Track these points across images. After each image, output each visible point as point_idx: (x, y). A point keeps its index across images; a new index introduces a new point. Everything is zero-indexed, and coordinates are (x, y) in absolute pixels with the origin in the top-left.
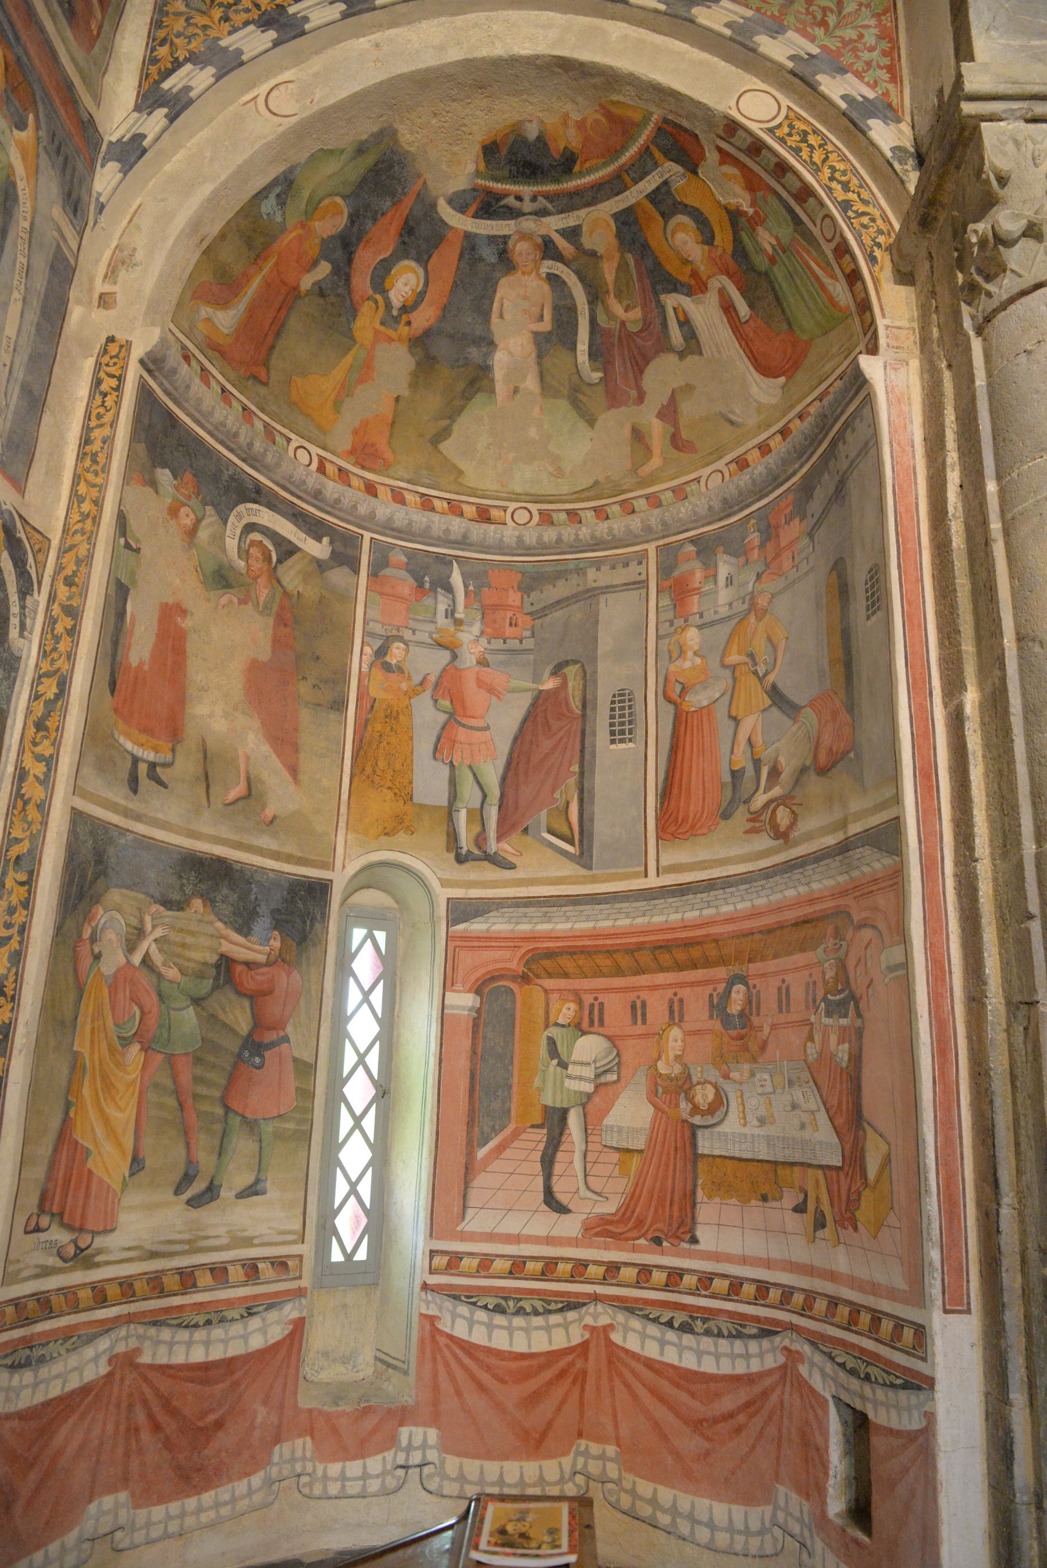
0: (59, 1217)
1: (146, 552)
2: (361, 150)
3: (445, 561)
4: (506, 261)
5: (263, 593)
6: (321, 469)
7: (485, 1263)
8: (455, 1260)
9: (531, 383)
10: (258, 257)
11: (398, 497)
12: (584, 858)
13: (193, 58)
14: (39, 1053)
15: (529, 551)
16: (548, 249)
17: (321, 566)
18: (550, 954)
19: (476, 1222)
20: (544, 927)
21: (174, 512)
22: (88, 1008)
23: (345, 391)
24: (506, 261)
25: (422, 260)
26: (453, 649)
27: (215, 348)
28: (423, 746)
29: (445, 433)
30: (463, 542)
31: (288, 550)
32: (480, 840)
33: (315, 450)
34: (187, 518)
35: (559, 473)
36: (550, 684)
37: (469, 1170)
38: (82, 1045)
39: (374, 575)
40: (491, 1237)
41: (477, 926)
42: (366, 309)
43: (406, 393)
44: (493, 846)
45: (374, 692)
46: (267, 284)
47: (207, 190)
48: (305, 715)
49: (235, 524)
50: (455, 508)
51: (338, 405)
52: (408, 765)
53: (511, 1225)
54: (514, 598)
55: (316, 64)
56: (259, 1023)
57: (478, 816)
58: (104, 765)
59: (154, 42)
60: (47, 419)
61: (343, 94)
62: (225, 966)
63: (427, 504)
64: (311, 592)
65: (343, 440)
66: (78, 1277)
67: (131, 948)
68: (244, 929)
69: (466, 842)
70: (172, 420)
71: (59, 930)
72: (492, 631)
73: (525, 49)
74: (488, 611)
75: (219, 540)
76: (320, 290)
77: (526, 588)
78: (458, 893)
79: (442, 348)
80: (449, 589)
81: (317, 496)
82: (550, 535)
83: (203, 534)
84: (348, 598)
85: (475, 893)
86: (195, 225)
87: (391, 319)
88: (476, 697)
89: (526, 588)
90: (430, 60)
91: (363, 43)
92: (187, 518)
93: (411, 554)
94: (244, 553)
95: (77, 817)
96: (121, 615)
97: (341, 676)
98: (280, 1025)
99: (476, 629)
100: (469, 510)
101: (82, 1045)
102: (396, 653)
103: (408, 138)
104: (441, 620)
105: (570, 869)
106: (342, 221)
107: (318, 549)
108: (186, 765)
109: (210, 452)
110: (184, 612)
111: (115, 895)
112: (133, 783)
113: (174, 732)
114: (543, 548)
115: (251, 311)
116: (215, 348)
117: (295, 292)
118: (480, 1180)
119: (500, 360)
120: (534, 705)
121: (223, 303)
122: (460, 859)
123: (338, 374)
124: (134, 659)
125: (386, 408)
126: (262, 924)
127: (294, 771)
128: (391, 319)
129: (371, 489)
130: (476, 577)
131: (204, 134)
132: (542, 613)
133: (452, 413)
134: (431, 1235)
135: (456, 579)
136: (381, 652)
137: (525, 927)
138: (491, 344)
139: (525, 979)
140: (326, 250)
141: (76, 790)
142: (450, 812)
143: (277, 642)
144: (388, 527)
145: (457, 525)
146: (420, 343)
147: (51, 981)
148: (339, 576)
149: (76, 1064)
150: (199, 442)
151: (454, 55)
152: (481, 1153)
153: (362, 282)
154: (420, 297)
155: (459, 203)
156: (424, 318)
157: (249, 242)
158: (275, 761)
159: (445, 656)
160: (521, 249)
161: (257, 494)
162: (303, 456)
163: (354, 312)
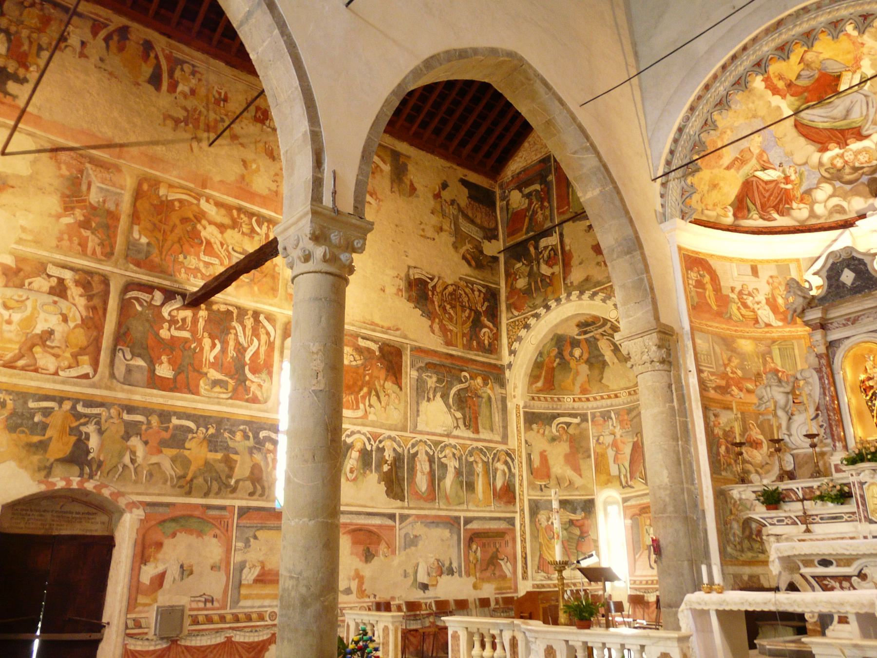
0: (543, 571)
1: (533, 444)
2: (552, 339)
3: (609, 411)
4: (597, 340)
5: (565, 437)
6: (574, 401)
7: (641, 582)
8: (635, 582)
9: (616, 360)
10: (542, 368)
11: (595, 399)
12: (646, 484)
13: (515, 341)
14: (531, 541)
15: (628, 403)
16: (603, 335)
17: (578, 424)
18: (644, 508)
19: (638, 573)
20: (642, 502)
21: (538, 432)
22: (541, 534)
23: (574, 380)
24: (597, 340)
25: (578, 346)
26: (613, 434)
27: (540, 391)
28: (611, 461)
29: (602, 378)
30: (612, 405)
31: (568, 424)
32: (627, 482)
33: (571, 397)
34: (541, 431)
35: (629, 381)
36: (635, 439)
37: (635, 561)
38: (541, 540)
39: (592, 421)
40: (641, 576)
41: (629, 503)
42: (571, 362)
43: (589, 373)
44: (629, 483)
45: (598, 451)
46: (546, 371)
47: (525, 367)
48: (581, 462)
49: (554, 425)
50: (609, 397)
51: (574, 384)
52: (608, 466)
53: (644, 573)
54: (626, 417)
55: (537, 329)
56: (582, 532)
57: (625, 476)
58: (534, 489)
59: (509, 338)
60: (509, 427)
61: (542, 336)
62: (571, 522)
63: (602, 398)
64: (577, 432)
65: (577, 389)
66: (549, 582)
67: (548, 521)
68: (574, 512)
69: (624, 483)
70: (533, 413)
71: (531, 521)
72: (622, 428)
73: (570, 314)
74: (621, 422)
75: (551, 432)
76: (559, 364)
77: (628, 414)
78: (624, 496)
79: (593, 360)
80: (611, 418)
81: (573, 409)
82: (632, 398)
83: (546, 432)
84: (587, 430)
85: (627, 495)
86: (525, 374)
87: (578, 360)
88: (621, 445)
89: (628, 414)
90: (555, 323)
91: (543, 322)
92: (541, 431)
93: (600, 412)
94: (557, 431)
95: (530, 500)
96: (530, 459)
97: (588, 450)
98: (587, 532)
99: (619, 427)
100: (613, 396)
101: (541, 540)
102: (601, 438)
103: (560, 332)
104: (611, 427)
105: (644, 487)
106: (556, 351)
107: (577, 420)
108: (553, 482)
109: (544, 414)
110: (545, 451)
111: (542, 512)
112: (541, 490)
113: (548, 476)
114: (628, 403)
115: (545, 378)
116: (540, 391)
117: (553, 369)
118: (638, 563)
119: (607, 358)
120: (633, 445)
121: (537, 382)
122: (623, 487)
123: (571, 377)
124: (535, 466)
125: (585, 379)
126: (579, 511)
127: (580, 475)
128: (578, 360)
129: (588, 400)
130: (617, 413)
131: (522, 353)
132: (631, 421)
133: (602, 373)
134: (630, 576)
135: (613, 415)
136: (598, 440)
137: (638, 502)
138: (603, 356)
139: (640, 515)
140: (556, 357)
141: (528, 495)
142: (620, 477)
143: (571, 447)
144: (593, 408)
145: (609, 402)
146: (587, 362)
147: (531, 530)
148: (584, 425)
149: (540, 544)
150: (541, 413)
151: (558, 320)
152: (637, 557)
153: (567, 357)
154: (582, 354)
155: (578, 335)
156: (586, 356)
157: (538, 367)
158: (575, 474)
159: (613, 437)
160: (598, 336)
161: (559, 415)
162: (569, 400)
163: (569, 363)
